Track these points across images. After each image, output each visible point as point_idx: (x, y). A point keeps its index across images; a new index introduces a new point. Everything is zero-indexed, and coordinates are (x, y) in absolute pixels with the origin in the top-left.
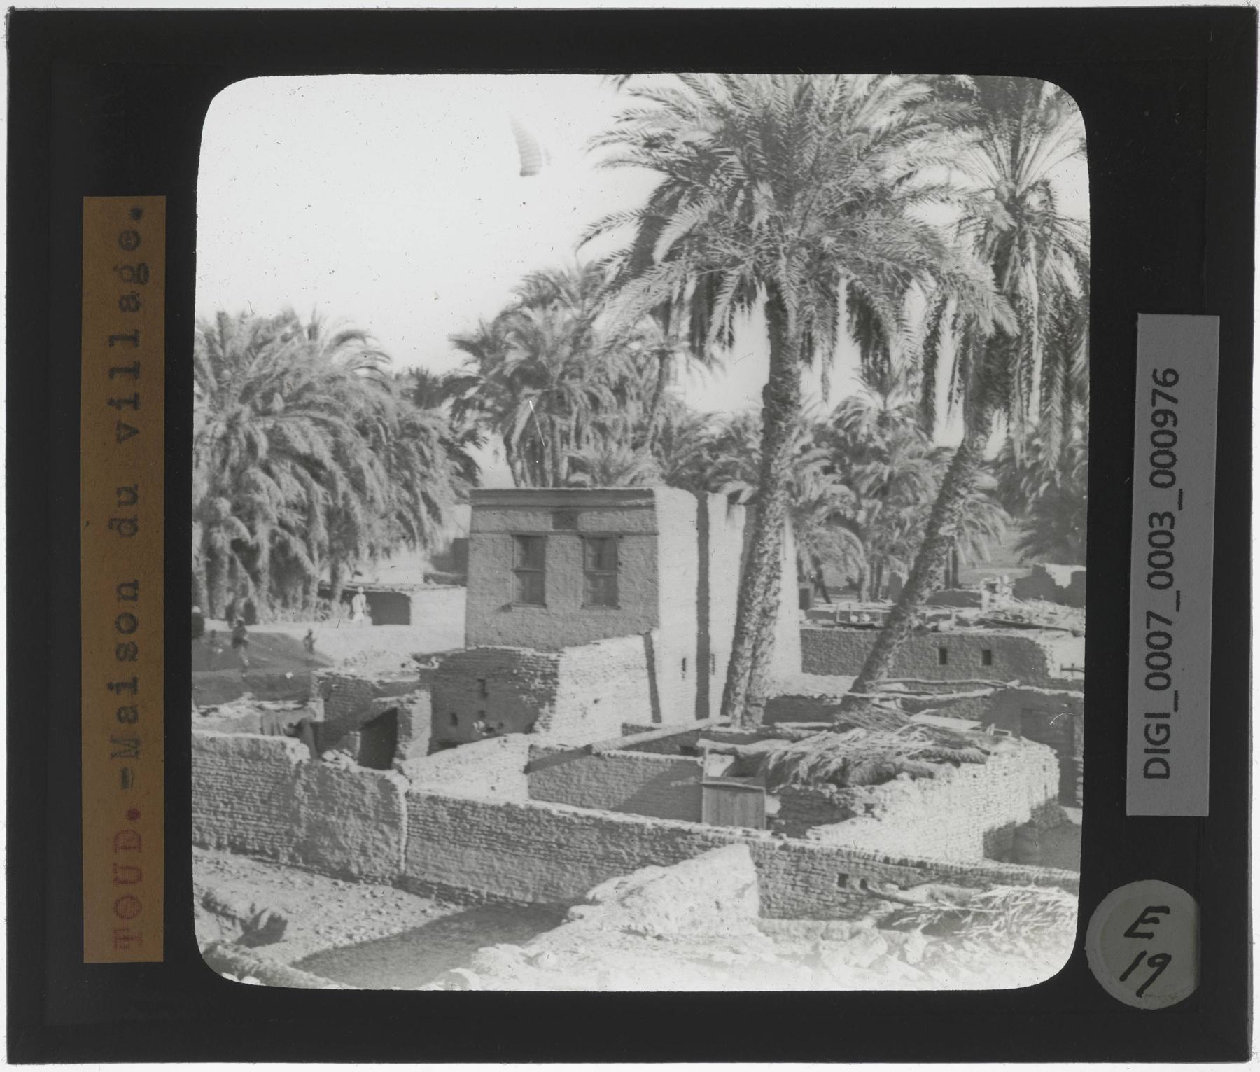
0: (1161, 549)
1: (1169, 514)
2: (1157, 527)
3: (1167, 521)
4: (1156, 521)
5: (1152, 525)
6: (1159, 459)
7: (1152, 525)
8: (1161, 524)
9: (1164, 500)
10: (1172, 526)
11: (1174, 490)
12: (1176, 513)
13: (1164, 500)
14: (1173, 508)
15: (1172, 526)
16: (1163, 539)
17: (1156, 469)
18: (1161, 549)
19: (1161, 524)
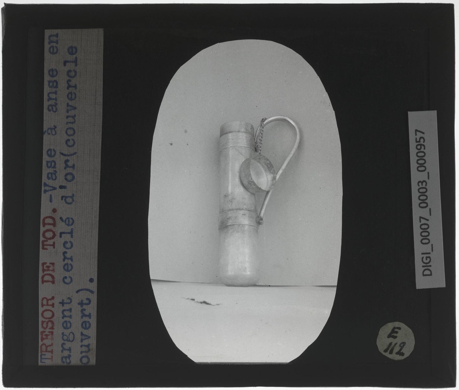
0: (423, 194)
1: (424, 181)
2: (421, 186)
3: (424, 184)
4: (420, 184)
5: (419, 186)
6: (420, 162)
7: (419, 186)
8: (422, 185)
9: (422, 176)
10: (426, 185)
11: (426, 173)
12: (427, 180)
13: (422, 176)
14: (426, 179)
15: (426, 185)
16: (424, 190)
17: (419, 165)
18: (423, 194)
19: (422, 185)
